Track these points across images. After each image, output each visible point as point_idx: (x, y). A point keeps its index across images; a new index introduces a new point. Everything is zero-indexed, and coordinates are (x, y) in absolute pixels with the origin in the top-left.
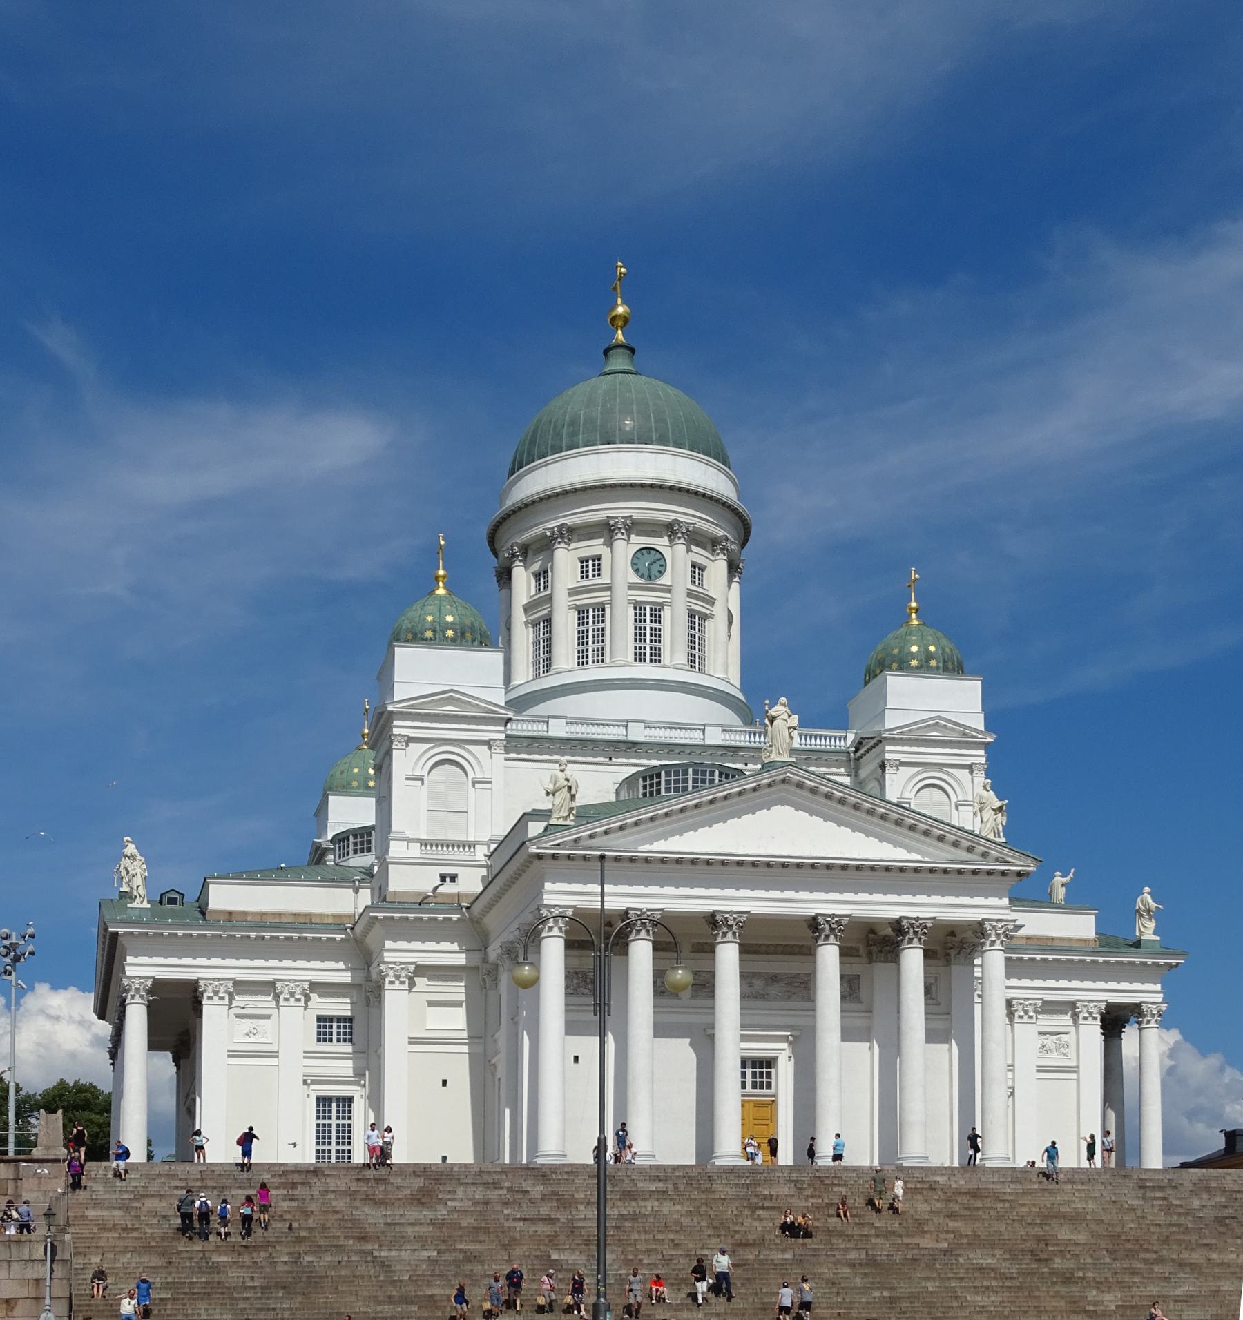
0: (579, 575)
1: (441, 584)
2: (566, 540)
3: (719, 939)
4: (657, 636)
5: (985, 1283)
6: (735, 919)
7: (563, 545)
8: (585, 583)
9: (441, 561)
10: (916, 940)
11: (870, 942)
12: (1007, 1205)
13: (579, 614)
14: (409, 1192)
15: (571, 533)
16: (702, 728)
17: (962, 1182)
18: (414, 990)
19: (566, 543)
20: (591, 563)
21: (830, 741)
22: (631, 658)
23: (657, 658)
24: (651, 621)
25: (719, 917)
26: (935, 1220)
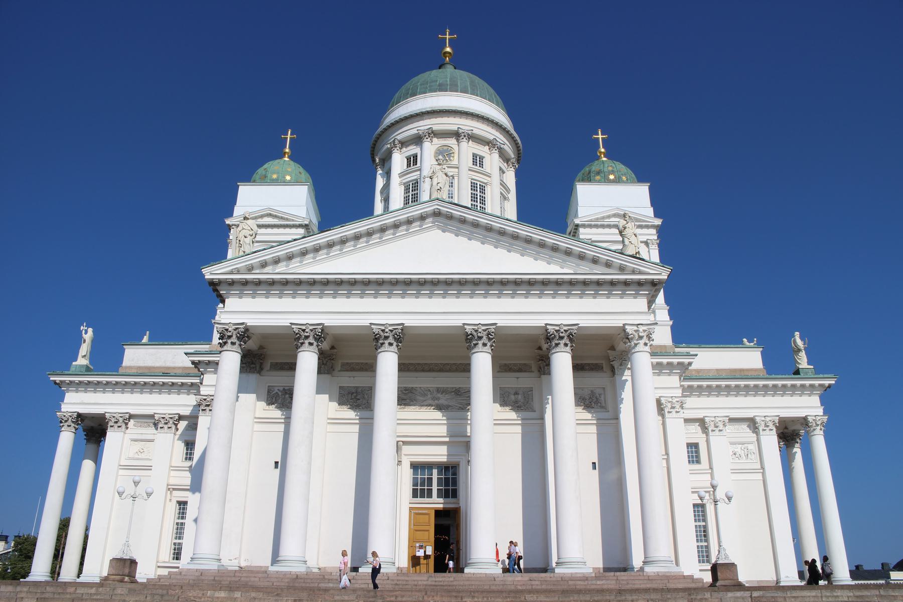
1: (287, 156)
2: (398, 148)
11: (538, 357)
13: (405, 187)
15: (404, 144)
19: (397, 150)
20: (412, 157)
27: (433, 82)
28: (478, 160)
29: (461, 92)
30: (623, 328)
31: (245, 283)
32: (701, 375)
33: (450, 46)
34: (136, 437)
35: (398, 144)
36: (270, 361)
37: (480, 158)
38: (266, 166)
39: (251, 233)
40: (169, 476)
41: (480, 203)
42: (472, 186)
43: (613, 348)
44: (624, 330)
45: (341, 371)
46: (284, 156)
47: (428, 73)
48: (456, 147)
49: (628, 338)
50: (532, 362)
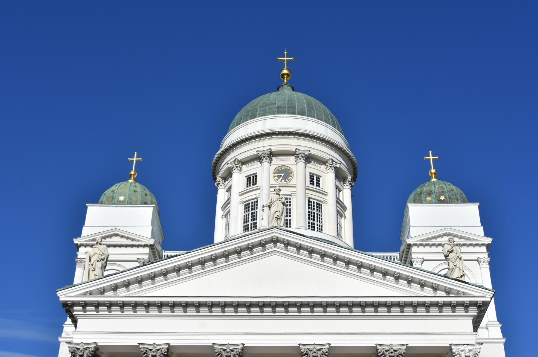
1: (132, 177)
13: (245, 205)
19: (238, 170)
27: (271, 104)
28: (315, 180)
29: (299, 114)
30: (449, 349)
31: (98, 305)
35: (239, 164)
37: (317, 178)
38: (113, 188)
39: (103, 257)
41: (317, 221)
42: (309, 205)
44: (451, 350)
47: (268, 95)
48: (294, 168)
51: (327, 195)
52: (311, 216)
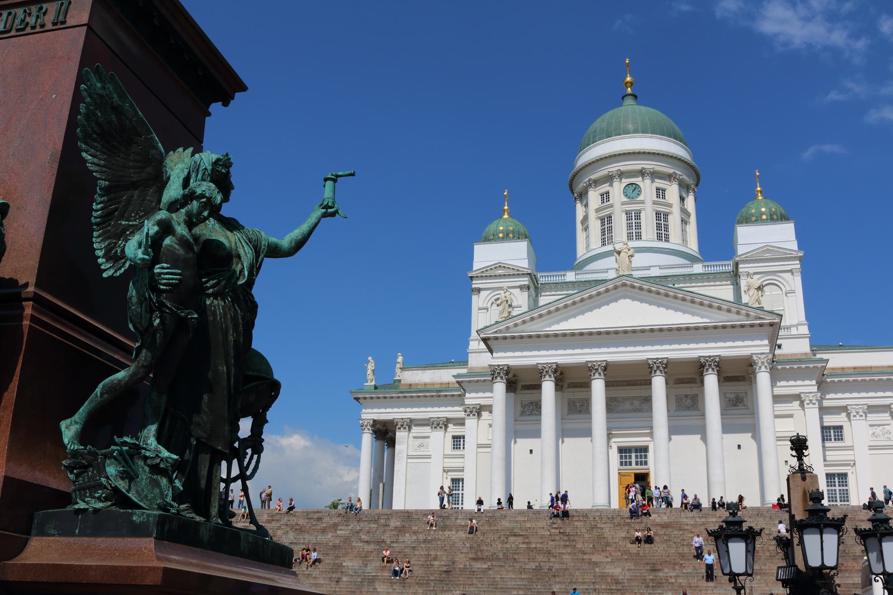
0: (601, 202)
1: (506, 213)
2: (593, 186)
3: (592, 378)
4: (639, 226)
5: (597, 586)
6: (599, 365)
7: (591, 189)
8: (604, 205)
9: (506, 203)
10: (710, 370)
12: (681, 532)
14: (325, 526)
15: (596, 183)
16: (648, 268)
17: (665, 518)
18: (481, 418)
19: (593, 188)
21: (719, 267)
22: (625, 239)
23: (639, 237)
24: (635, 219)
25: (590, 365)
26: (620, 543)
28: (661, 192)
31: (505, 338)
32: (843, 372)
33: (630, 76)
34: (415, 435)
36: (520, 384)
37: (662, 190)
40: (444, 462)
43: (751, 365)
45: (568, 388)
46: (504, 214)
49: (754, 362)
50: (697, 376)
51: (671, 207)
52: (659, 227)
